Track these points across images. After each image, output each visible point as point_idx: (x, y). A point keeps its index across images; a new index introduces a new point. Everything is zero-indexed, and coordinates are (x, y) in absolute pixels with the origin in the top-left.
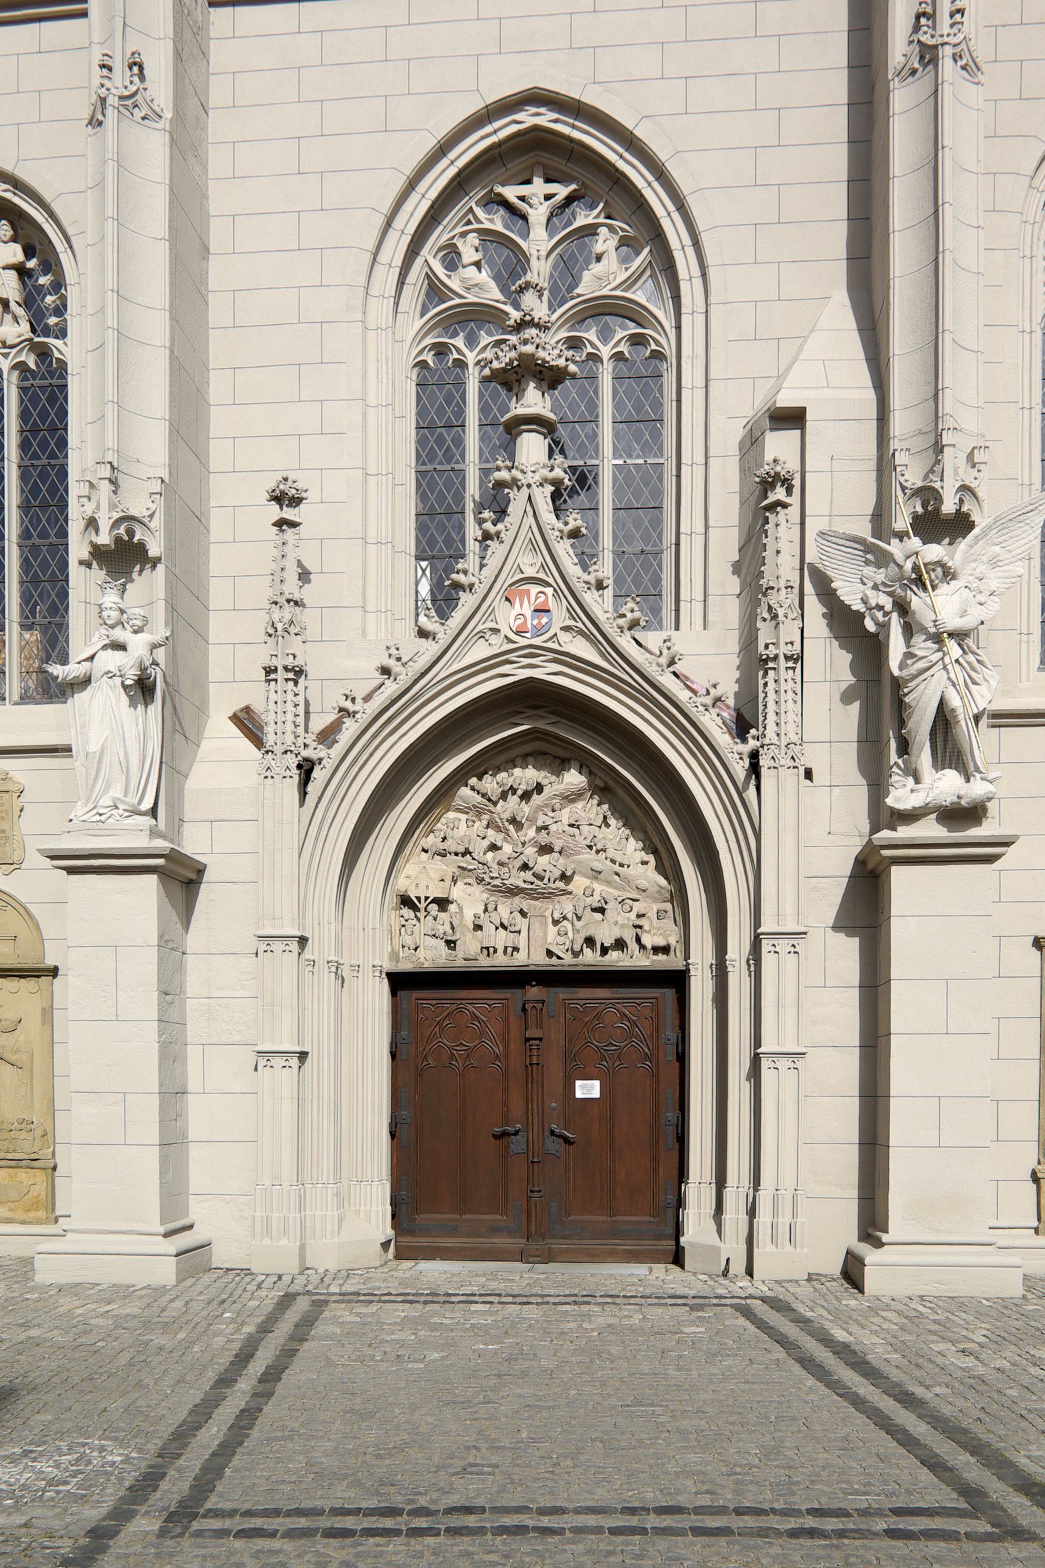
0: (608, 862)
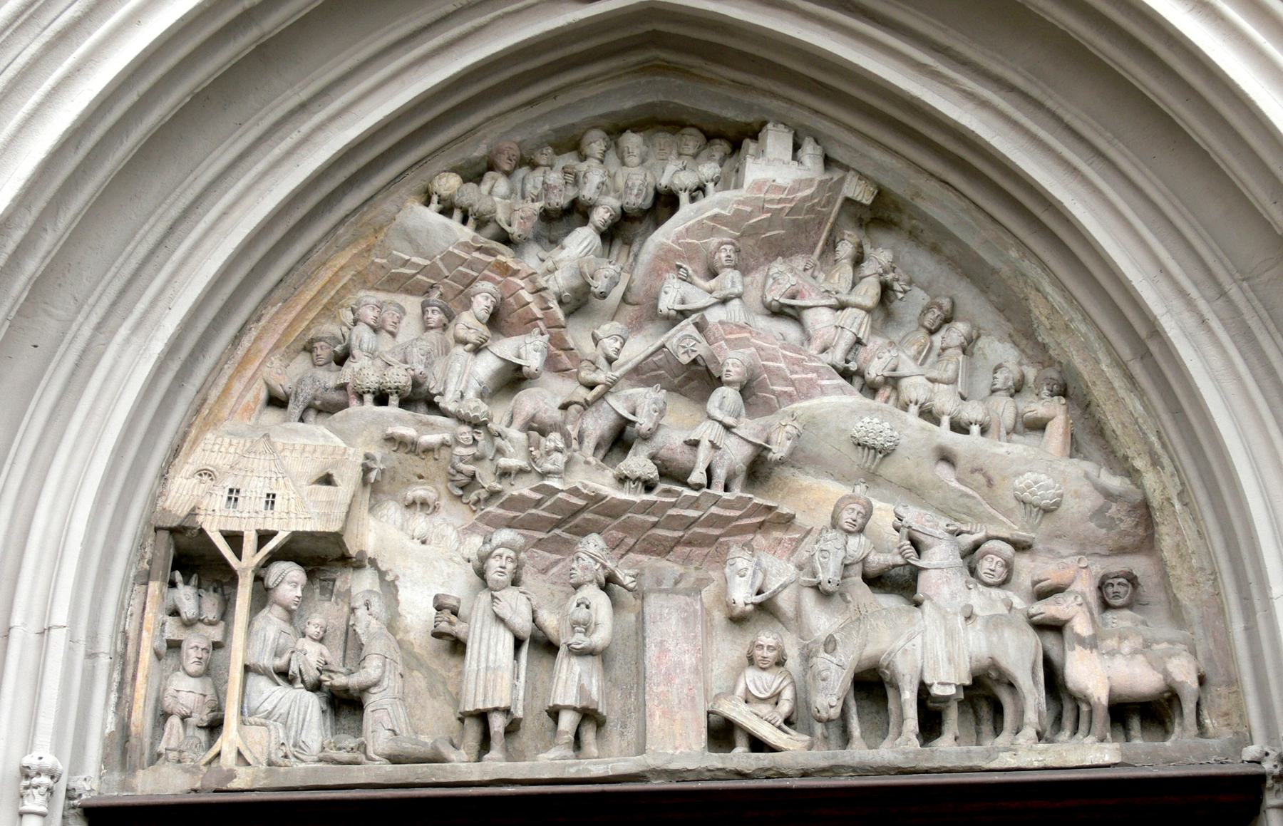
0: (912, 416)
